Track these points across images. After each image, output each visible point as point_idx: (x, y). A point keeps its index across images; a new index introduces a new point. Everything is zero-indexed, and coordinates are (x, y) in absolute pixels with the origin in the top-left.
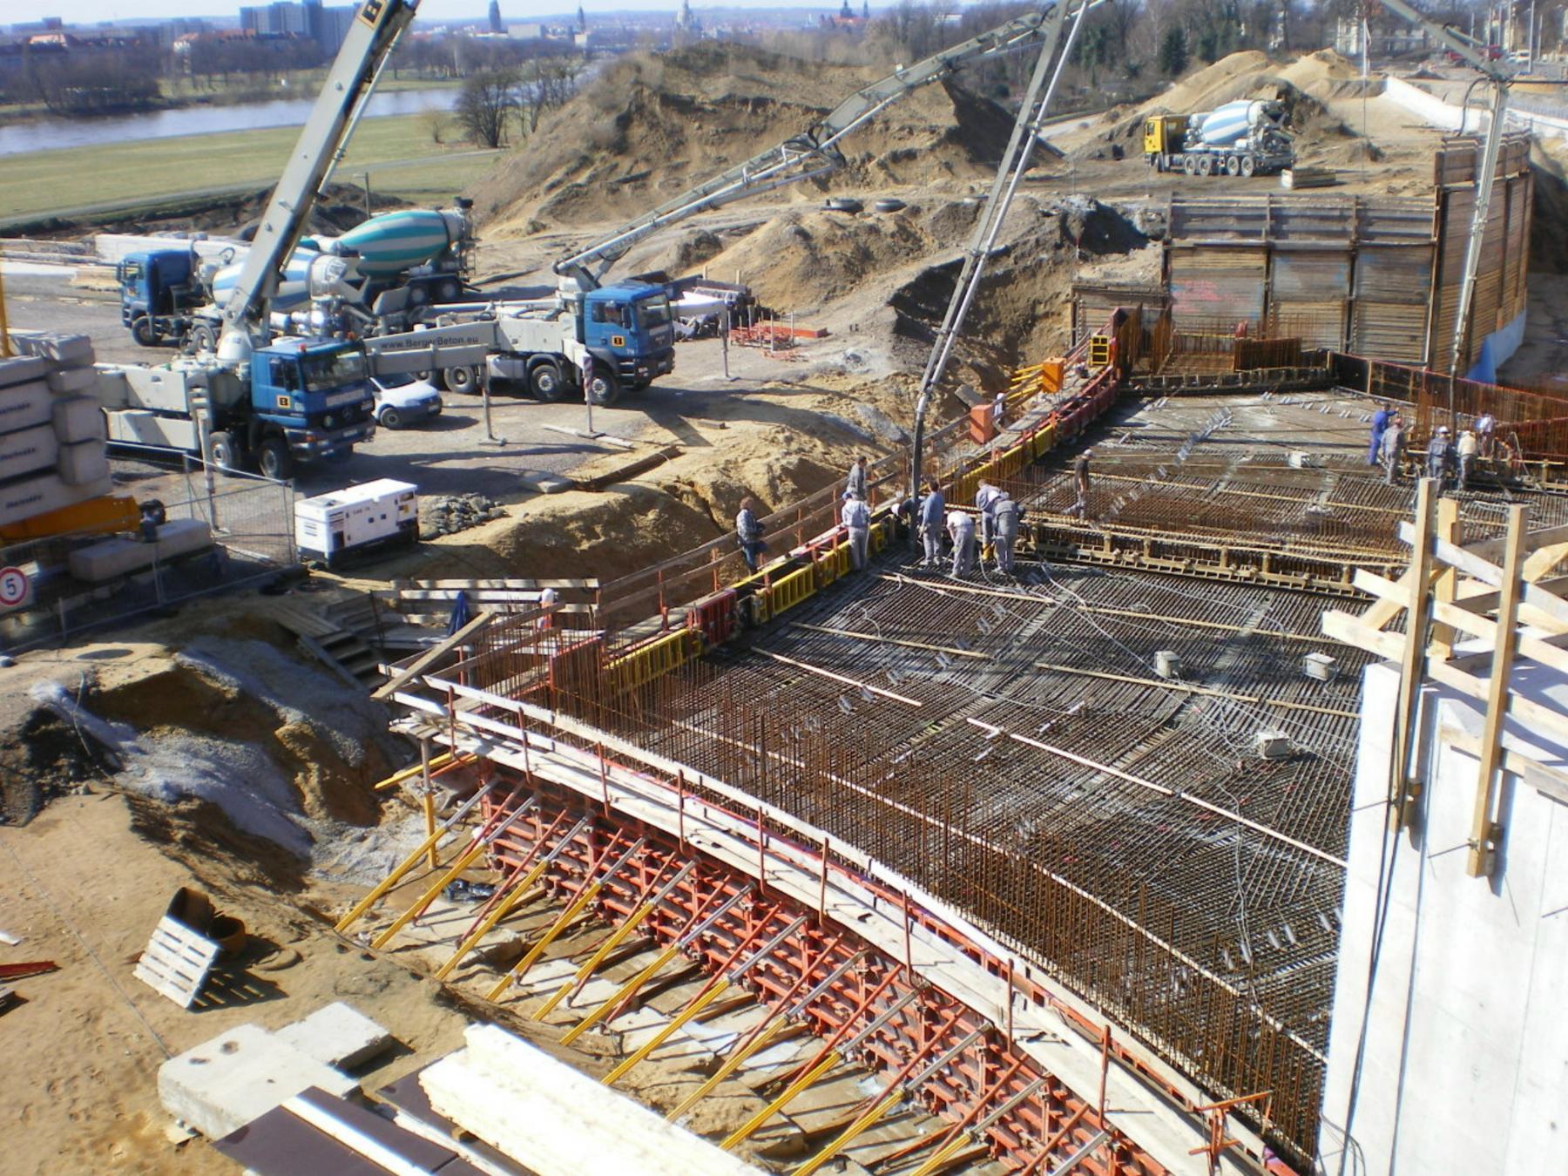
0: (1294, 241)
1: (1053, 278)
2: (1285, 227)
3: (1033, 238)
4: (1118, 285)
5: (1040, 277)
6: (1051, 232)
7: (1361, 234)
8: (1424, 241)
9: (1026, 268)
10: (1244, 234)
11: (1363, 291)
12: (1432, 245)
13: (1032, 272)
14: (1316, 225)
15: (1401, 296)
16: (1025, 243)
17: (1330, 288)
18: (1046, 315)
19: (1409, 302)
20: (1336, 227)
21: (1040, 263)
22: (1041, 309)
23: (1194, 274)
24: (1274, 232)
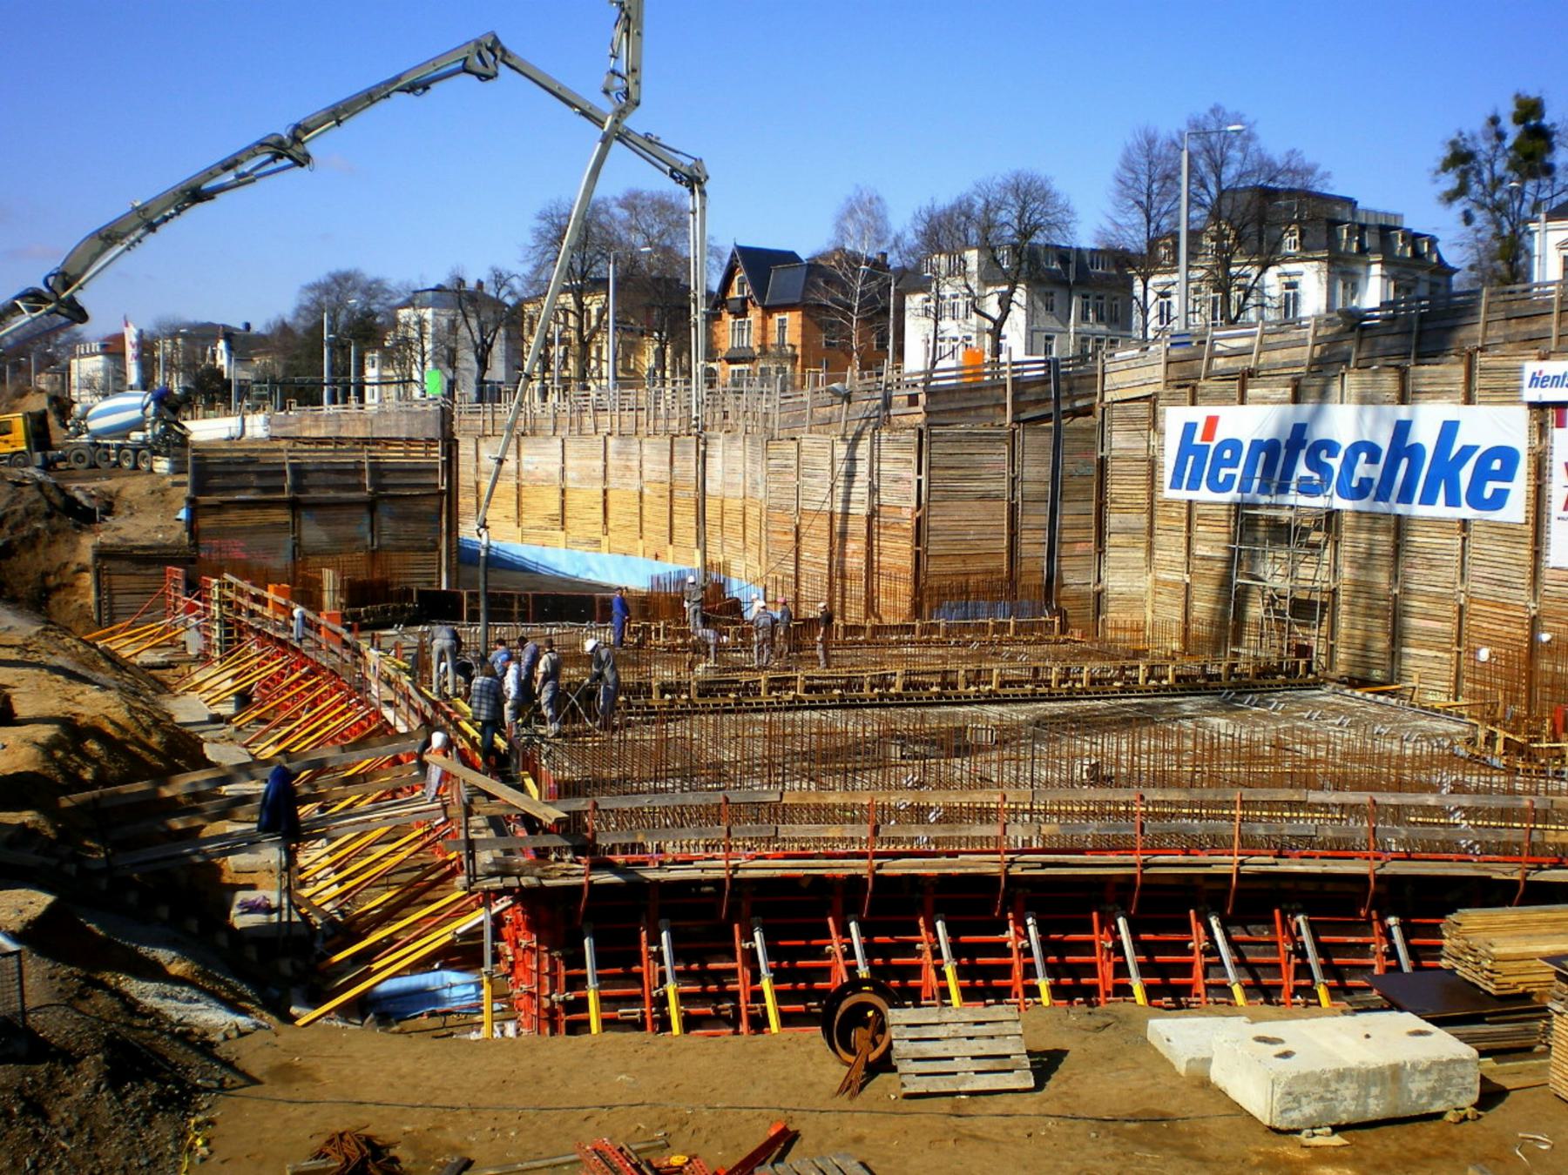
0: (314, 494)
1: (55, 549)
2: (305, 482)
3: (20, 507)
4: (144, 548)
5: (40, 549)
6: (37, 501)
7: (377, 486)
8: (432, 491)
9: (24, 539)
10: (266, 490)
11: (384, 541)
12: (441, 493)
13: (32, 541)
14: (333, 478)
15: (417, 544)
16: (14, 512)
17: (354, 540)
18: (58, 588)
19: (424, 550)
20: (352, 480)
21: (36, 534)
22: (52, 581)
23: (222, 532)
24: (297, 487)
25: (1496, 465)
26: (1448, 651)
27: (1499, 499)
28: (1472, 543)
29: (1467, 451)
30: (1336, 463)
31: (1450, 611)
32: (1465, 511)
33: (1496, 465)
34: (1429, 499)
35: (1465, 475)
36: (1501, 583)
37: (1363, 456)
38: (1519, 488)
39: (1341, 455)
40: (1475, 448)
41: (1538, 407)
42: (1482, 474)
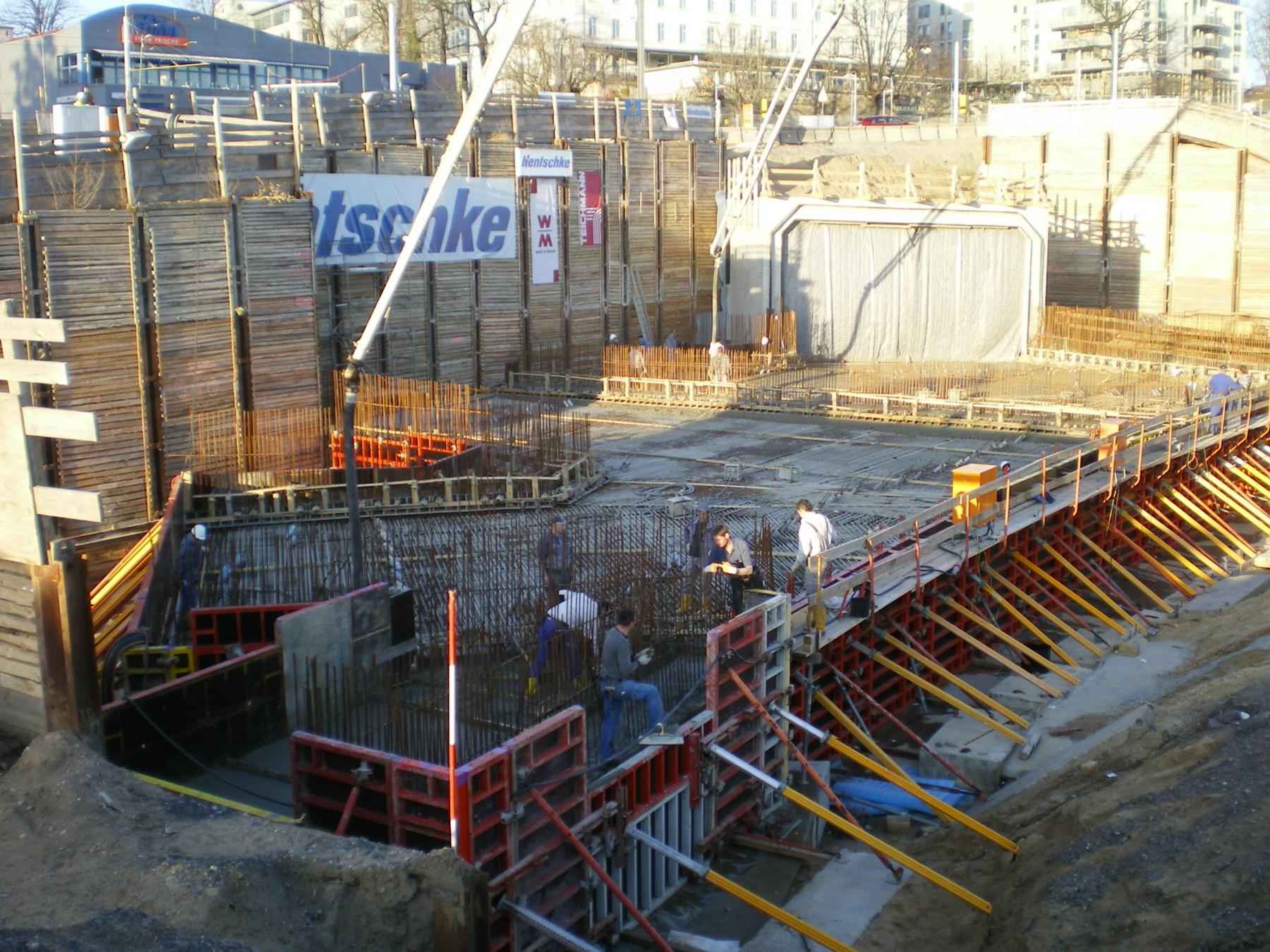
25: (496, 220)
26: (470, 356)
27: (499, 243)
28: (482, 277)
29: (476, 212)
30: (377, 225)
31: (468, 328)
32: (478, 254)
33: (496, 220)
34: (451, 248)
35: (476, 228)
36: (504, 301)
37: (399, 217)
38: (511, 234)
39: (381, 216)
40: (481, 209)
41: (523, 180)
42: (487, 227)
